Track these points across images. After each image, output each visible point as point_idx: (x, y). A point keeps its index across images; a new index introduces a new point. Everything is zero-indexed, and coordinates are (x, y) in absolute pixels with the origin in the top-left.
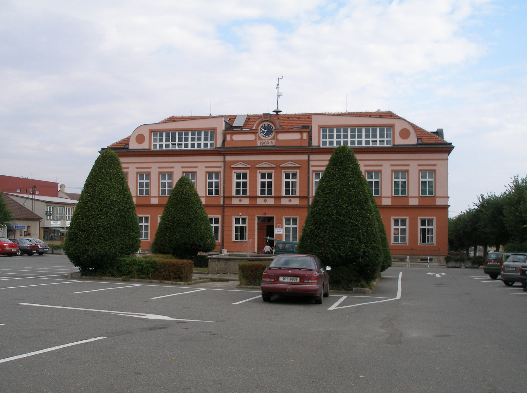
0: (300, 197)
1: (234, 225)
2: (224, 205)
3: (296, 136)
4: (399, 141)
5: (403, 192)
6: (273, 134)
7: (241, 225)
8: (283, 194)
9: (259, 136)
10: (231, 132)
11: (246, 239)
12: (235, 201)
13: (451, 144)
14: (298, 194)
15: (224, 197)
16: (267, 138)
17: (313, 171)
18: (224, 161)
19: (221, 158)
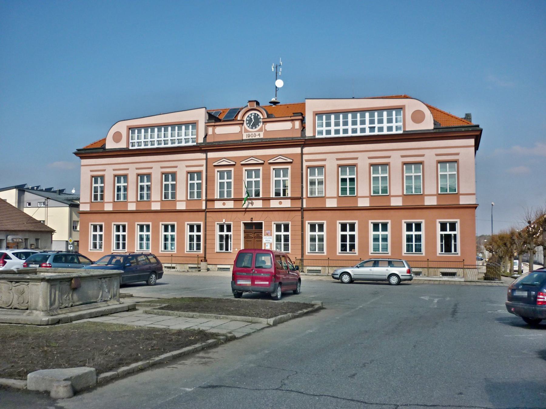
0: (292, 199)
1: (218, 233)
3: (287, 125)
4: (412, 127)
5: (352, 190)
6: (261, 124)
9: (245, 128)
10: (213, 124)
13: (478, 126)
15: (207, 200)
16: (254, 130)
17: (308, 167)
18: (207, 159)
19: (203, 156)
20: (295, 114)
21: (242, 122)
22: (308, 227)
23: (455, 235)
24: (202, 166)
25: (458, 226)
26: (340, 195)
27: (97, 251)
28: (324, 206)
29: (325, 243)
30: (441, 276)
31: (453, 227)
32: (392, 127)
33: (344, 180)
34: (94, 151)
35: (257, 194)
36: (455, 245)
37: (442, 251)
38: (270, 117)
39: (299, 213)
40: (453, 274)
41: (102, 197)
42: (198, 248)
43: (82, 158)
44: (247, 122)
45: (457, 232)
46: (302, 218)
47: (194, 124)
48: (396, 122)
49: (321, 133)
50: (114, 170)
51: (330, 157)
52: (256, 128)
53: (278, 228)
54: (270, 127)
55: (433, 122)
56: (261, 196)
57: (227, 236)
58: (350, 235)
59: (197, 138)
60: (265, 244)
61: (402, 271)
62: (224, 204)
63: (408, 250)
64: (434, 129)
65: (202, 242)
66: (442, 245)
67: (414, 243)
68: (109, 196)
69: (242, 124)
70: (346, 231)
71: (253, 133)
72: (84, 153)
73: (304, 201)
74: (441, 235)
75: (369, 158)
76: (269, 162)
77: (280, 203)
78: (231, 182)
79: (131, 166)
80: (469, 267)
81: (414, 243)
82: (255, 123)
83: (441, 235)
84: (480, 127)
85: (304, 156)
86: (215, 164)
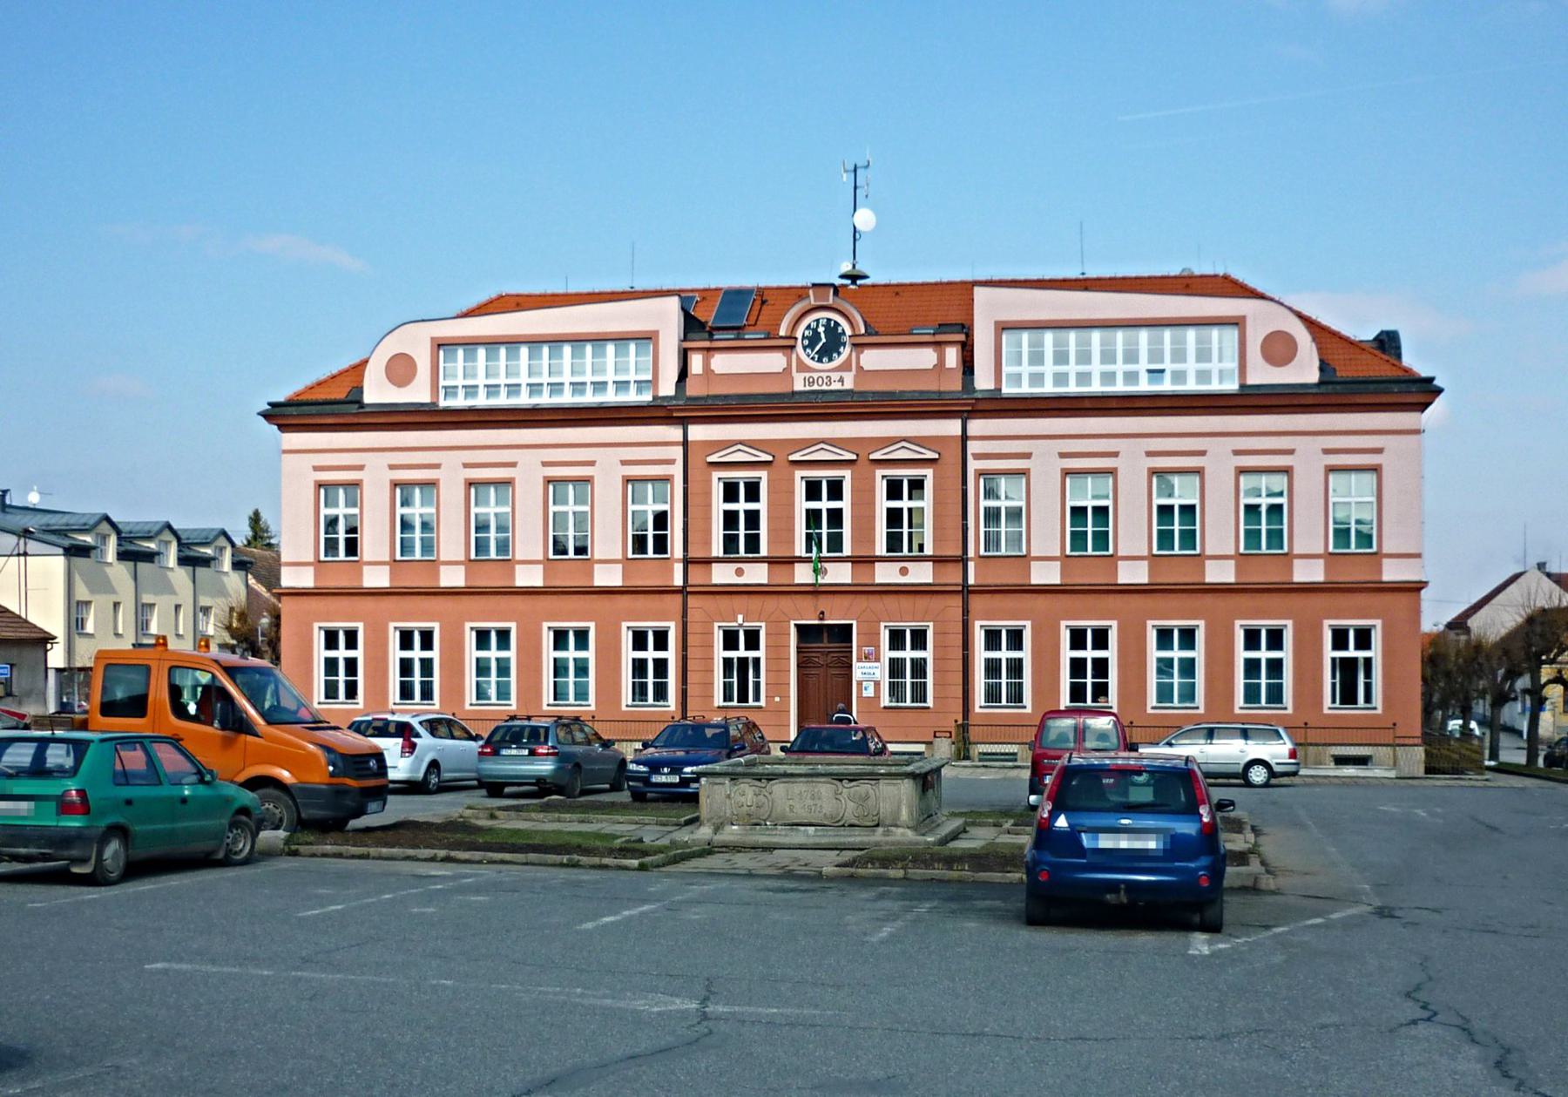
0: (937, 560)
1: (720, 654)
2: (684, 587)
3: (924, 358)
4: (1263, 374)
5: (1275, 537)
6: (846, 351)
7: (742, 652)
8: (881, 549)
9: (798, 358)
10: (707, 344)
11: (757, 698)
12: (722, 575)
13: (1431, 380)
14: (928, 551)
15: (687, 562)
16: (826, 365)
17: (980, 473)
18: (685, 443)
19: (675, 433)
20: (943, 327)
21: (791, 342)
22: (979, 638)
23: (1368, 661)
24: (671, 462)
25: (1377, 638)
26: (1068, 552)
27: (341, 704)
30: (1332, 765)
31: (1364, 639)
32: (1067, 374)
33: (1165, 511)
34: (328, 408)
35: (753, 543)
36: (1368, 687)
37: (1334, 701)
38: (874, 337)
40: (1362, 761)
41: (352, 547)
42: (661, 693)
43: (283, 428)
44: (806, 342)
45: (1375, 653)
46: (966, 611)
47: (647, 338)
48: (1220, 360)
49: (1017, 379)
50: (392, 467)
51: (1044, 447)
52: (831, 360)
53: (897, 639)
54: (873, 359)
55: (1317, 363)
56: (764, 552)
57: (743, 662)
58: (1095, 660)
59: (654, 382)
60: (860, 683)
61: (1277, 751)
62: (739, 572)
63: (1160, 698)
64: (1321, 383)
65: (672, 680)
66: (1334, 685)
68: (375, 544)
69: (793, 347)
70: (1085, 648)
71: (824, 375)
72: (286, 415)
73: (971, 565)
74: (1334, 660)
75: (1149, 454)
76: (792, 458)
77: (739, 572)
78: (757, 512)
79: (450, 456)
80: (1407, 741)
82: (829, 344)
83: (1334, 660)
84: (1436, 382)
85: (969, 443)
86: (713, 458)
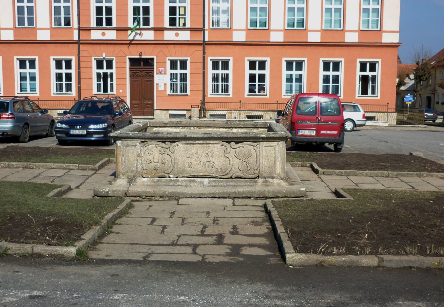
0: (192, 30)
1: (95, 71)
2: (79, 41)
7: (105, 70)
8: (167, 24)
11: (112, 90)
12: (96, 35)
14: (188, 25)
15: (80, 29)
22: (210, 65)
28: (229, 40)
29: (188, 82)
31: (373, 67)
35: (109, 21)
39: (201, 48)
42: (69, 88)
46: (204, 53)
53: (173, 65)
57: (105, 75)
67: (257, 83)
73: (207, 32)
81: (257, 83)
